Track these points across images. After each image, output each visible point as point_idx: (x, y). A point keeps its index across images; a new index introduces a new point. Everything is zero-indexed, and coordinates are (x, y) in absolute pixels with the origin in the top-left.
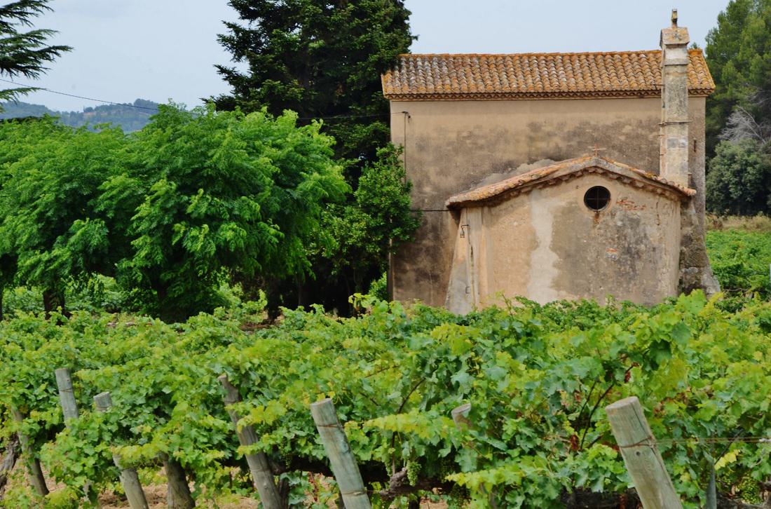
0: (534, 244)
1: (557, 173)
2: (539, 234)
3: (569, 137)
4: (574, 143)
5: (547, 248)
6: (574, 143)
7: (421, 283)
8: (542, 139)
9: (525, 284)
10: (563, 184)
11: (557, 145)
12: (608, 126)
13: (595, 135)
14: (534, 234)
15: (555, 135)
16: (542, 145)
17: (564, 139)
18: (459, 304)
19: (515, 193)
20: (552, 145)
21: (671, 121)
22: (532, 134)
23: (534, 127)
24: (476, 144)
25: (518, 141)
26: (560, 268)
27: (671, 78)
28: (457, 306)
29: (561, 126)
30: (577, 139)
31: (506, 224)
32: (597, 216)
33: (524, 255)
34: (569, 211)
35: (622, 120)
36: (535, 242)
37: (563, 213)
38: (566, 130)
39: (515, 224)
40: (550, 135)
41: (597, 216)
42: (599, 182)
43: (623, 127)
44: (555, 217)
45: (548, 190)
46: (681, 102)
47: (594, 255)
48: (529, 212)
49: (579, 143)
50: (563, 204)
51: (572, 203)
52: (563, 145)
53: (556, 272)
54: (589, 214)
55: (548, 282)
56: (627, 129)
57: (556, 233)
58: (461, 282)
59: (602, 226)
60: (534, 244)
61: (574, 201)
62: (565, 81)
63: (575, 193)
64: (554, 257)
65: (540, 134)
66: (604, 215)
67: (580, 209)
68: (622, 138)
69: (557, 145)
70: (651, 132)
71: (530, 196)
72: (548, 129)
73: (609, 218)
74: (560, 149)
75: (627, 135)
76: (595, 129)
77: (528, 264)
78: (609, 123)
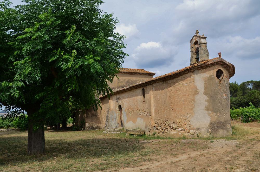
0: (196, 92)
1: (208, 63)
2: (198, 88)
3: (126, 83)
4: (127, 84)
5: (203, 94)
6: (127, 84)
7: (93, 117)
8: (120, 83)
9: (192, 109)
10: (208, 68)
11: (124, 84)
14: (196, 88)
15: (123, 82)
16: (120, 84)
17: (125, 83)
18: (111, 121)
19: (188, 72)
20: (123, 84)
21: (205, 59)
22: (118, 82)
26: (208, 102)
27: (203, 47)
28: (110, 122)
29: (125, 80)
30: (128, 83)
31: (181, 85)
32: (220, 81)
33: (191, 97)
34: (210, 79)
35: (137, 79)
36: (197, 91)
37: (208, 79)
38: (126, 81)
39: (186, 85)
40: (122, 82)
41: (220, 81)
42: (221, 68)
44: (205, 81)
46: (207, 54)
47: (220, 96)
48: (194, 79)
49: (128, 84)
50: (208, 76)
52: (125, 84)
53: (207, 103)
54: (217, 80)
55: (203, 108)
57: (206, 88)
58: (111, 116)
59: (222, 85)
60: (196, 92)
61: (212, 75)
63: (212, 72)
64: (206, 97)
66: (222, 81)
67: (215, 78)
69: (124, 84)
73: (223, 82)
74: (124, 85)
76: (132, 81)
77: (194, 100)
78: (134, 80)
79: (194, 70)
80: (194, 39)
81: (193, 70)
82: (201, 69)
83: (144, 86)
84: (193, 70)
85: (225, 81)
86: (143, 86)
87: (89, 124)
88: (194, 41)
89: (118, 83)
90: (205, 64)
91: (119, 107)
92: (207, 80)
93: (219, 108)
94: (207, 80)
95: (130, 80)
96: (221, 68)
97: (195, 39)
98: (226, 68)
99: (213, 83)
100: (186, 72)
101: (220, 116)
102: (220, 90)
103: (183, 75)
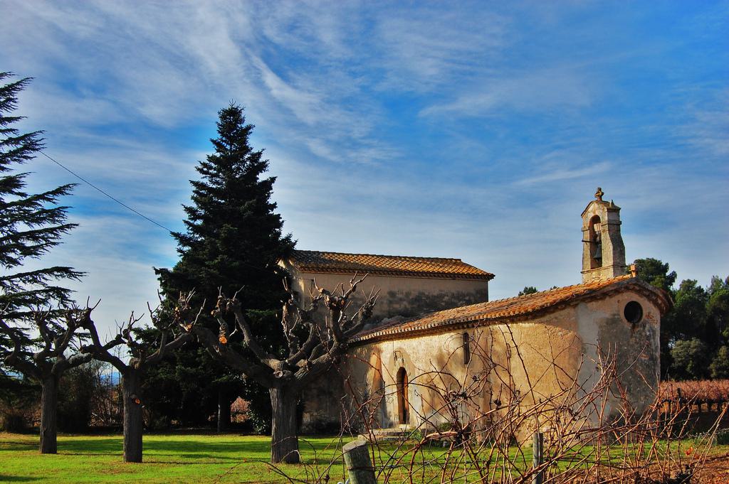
7: (321, 397)
8: (397, 303)
10: (607, 298)
11: (405, 306)
12: (435, 296)
13: (428, 301)
15: (404, 300)
16: (397, 306)
17: (409, 303)
19: (563, 306)
20: (402, 306)
22: (391, 299)
23: (392, 294)
24: (357, 303)
25: (382, 303)
29: (408, 294)
32: (634, 327)
34: (613, 321)
37: (607, 323)
38: (411, 298)
40: (401, 299)
42: (635, 297)
43: (443, 297)
45: (594, 304)
49: (419, 306)
50: (608, 315)
51: (614, 315)
54: (628, 326)
56: (446, 298)
61: (615, 312)
62: (399, 266)
65: (396, 299)
68: (443, 304)
69: (405, 306)
70: (459, 301)
71: (576, 309)
72: (400, 296)
75: (445, 302)
76: (428, 297)
79: (576, 303)
80: (590, 209)
81: (575, 303)
82: (591, 302)
83: (468, 327)
84: (575, 303)
85: (644, 327)
86: (465, 326)
87: (312, 415)
88: (590, 215)
89: (391, 302)
90: (601, 291)
91: (398, 373)
92: (604, 324)
93: (630, 384)
94: (604, 324)
95: (423, 294)
96: (635, 297)
97: (594, 213)
98: (648, 297)
99: (616, 332)
100: (559, 307)
101: (632, 401)
102: (632, 346)
103: (553, 312)
